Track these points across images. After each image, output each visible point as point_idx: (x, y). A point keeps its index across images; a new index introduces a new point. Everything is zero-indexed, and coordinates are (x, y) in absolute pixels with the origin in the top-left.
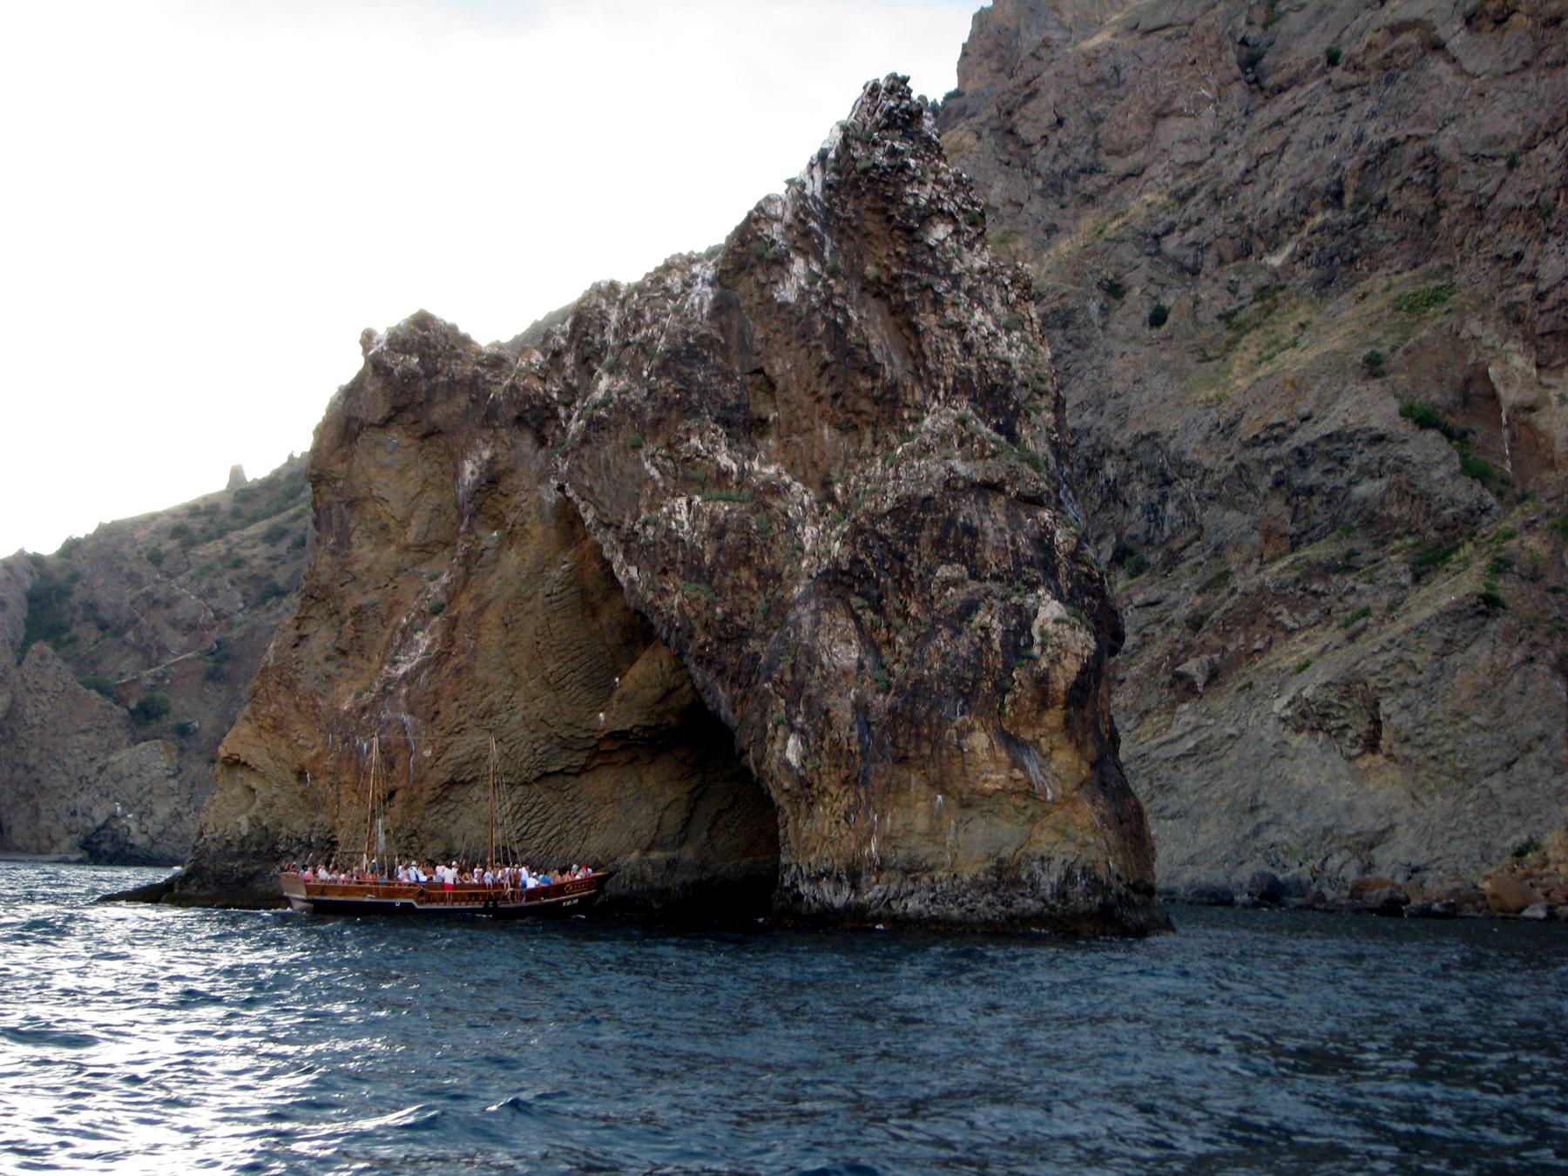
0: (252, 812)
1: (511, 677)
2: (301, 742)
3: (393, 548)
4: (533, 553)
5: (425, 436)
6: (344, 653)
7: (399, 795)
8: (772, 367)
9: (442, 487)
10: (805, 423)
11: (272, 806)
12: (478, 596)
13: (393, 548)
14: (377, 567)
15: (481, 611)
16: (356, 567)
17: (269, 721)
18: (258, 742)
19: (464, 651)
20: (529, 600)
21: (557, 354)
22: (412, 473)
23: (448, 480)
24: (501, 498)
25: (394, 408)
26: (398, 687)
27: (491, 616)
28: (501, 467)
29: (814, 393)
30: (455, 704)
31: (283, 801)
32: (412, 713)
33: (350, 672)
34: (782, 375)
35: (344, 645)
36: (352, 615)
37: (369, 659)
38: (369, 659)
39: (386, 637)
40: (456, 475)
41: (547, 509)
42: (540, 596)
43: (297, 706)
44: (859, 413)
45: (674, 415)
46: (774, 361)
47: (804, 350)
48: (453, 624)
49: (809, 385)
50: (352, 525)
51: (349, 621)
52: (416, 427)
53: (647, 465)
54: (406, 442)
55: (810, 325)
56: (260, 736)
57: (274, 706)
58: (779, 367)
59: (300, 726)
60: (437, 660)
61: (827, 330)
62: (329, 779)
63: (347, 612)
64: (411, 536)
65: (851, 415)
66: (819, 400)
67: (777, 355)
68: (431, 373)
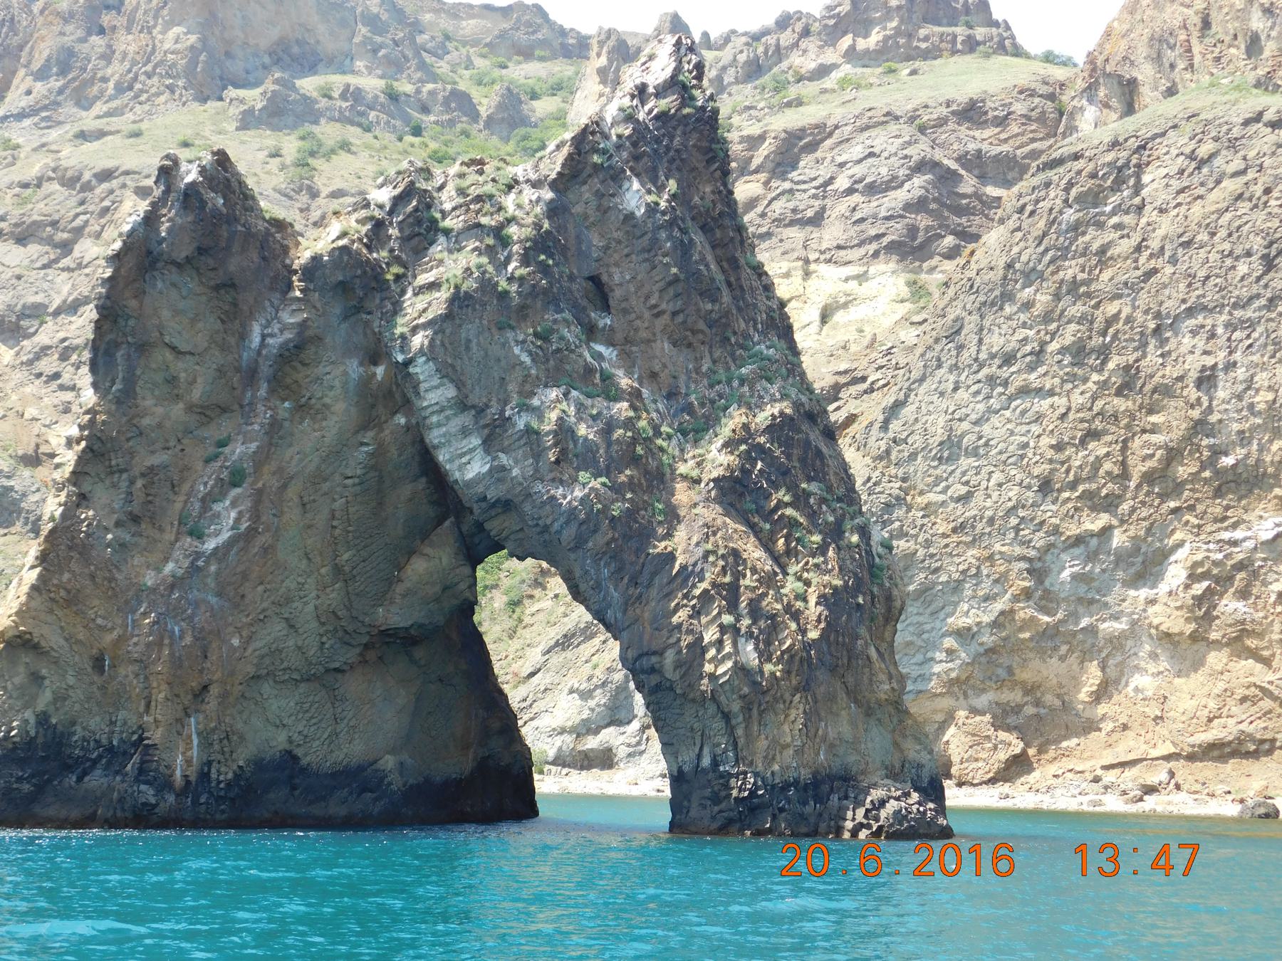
0: (41, 706)
1: (305, 561)
2: (99, 621)
3: (181, 405)
4: (334, 431)
5: (217, 288)
6: (135, 519)
7: (215, 690)
8: (610, 275)
9: (224, 348)
10: (644, 334)
11: (65, 699)
12: (280, 470)
13: (181, 405)
14: (168, 424)
15: (284, 487)
16: (146, 421)
17: (63, 593)
18: (50, 618)
19: (267, 529)
20: (325, 480)
21: (379, 225)
22: (200, 325)
23: (232, 340)
24: (299, 366)
25: (199, 249)
26: (207, 562)
27: (292, 493)
28: (310, 333)
29: (655, 306)
30: (260, 588)
31: (77, 694)
32: (219, 594)
33: (143, 542)
34: (621, 285)
35: (136, 507)
36: (143, 475)
37: (161, 529)
38: (161, 529)
39: (178, 506)
40: (243, 336)
41: (351, 386)
42: (337, 478)
43: (93, 577)
44: (694, 332)
45: (539, 304)
46: (613, 269)
47: (646, 265)
48: (259, 495)
49: (647, 297)
50: (138, 372)
51: (139, 483)
52: (212, 274)
53: (517, 350)
54: (199, 290)
55: (655, 244)
56: (51, 611)
57: (66, 576)
58: (617, 277)
59: (96, 602)
60: (242, 539)
61: (674, 248)
62: (136, 668)
63: (136, 471)
64: (196, 394)
65: (688, 333)
66: (657, 315)
67: (617, 265)
68: (231, 219)
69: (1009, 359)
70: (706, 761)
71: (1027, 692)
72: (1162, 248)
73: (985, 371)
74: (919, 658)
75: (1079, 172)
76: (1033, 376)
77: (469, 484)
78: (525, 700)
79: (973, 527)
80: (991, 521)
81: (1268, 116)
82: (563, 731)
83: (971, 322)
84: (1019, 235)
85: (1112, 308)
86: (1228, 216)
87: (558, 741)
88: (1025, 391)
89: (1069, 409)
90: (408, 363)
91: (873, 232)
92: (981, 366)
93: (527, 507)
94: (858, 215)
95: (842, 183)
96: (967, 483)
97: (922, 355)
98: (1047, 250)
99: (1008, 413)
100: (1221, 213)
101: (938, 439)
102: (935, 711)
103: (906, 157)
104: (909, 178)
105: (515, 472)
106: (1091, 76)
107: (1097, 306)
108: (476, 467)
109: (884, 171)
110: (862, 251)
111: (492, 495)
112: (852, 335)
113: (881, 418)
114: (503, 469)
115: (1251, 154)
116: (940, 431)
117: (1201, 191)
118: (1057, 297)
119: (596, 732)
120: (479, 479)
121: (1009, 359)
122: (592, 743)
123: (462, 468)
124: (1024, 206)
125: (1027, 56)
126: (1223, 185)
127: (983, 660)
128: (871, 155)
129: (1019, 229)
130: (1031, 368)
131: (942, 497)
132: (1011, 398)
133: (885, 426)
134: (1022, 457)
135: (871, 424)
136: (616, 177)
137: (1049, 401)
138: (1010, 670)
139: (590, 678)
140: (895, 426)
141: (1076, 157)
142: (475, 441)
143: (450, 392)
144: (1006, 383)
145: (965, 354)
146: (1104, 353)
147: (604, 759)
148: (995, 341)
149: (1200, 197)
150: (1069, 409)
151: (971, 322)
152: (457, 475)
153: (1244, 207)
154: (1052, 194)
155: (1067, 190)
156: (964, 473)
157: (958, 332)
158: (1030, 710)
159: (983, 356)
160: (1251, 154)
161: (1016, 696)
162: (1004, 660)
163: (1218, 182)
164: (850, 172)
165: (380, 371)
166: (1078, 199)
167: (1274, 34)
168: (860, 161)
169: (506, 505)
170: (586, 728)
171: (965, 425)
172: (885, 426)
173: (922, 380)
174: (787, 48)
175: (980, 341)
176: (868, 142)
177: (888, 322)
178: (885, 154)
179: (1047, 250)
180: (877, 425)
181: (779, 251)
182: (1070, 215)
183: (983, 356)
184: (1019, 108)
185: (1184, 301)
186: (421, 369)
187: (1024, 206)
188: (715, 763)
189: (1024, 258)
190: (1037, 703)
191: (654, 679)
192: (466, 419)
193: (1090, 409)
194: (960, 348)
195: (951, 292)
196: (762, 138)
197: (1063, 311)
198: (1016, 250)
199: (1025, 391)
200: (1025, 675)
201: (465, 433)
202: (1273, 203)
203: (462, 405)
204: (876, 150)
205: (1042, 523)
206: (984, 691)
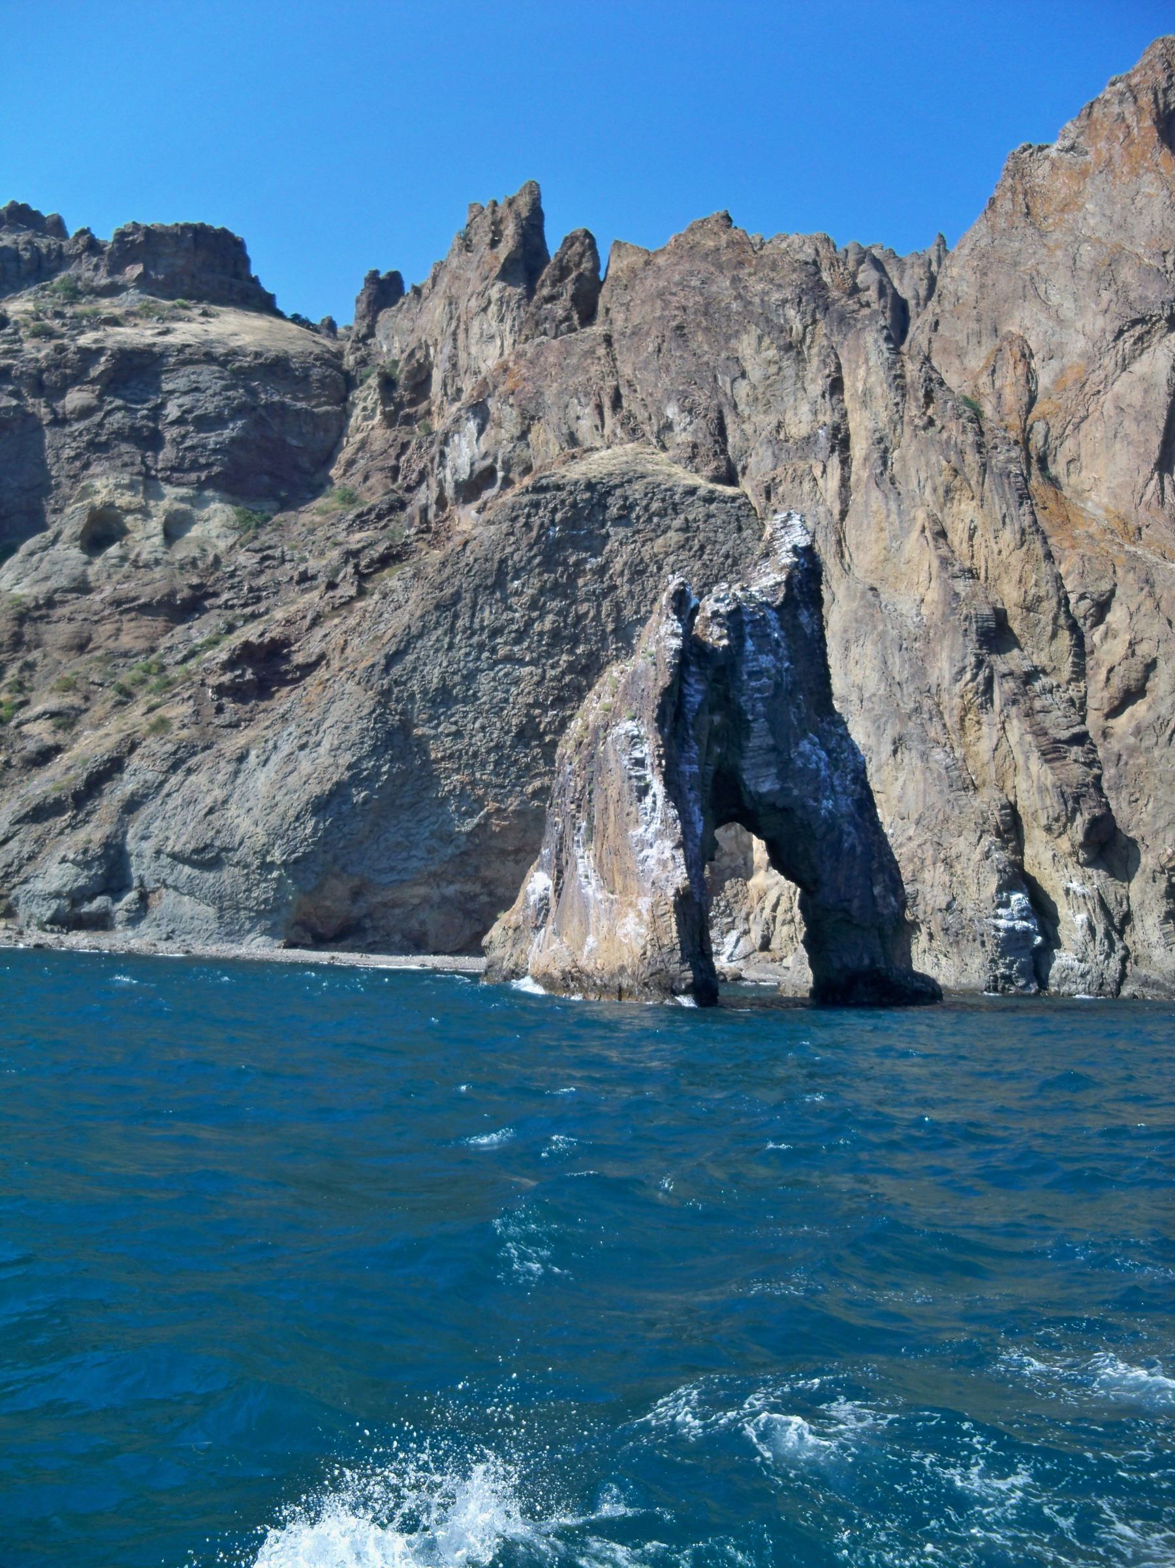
69: (496, 632)
70: (866, 961)
71: (484, 885)
72: (622, 572)
73: (475, 639)
74: (404, 854)
75: (563, 502)
76: (516, 649)
77: (761, 795)
78: (10, 865)
79: (460, 757)
80: (475, 755)
81: (702, 492)
82: (57, 895)
83: (467, 598)
84: (512, 539)
85: (583, 608)
86: (672, 558)
87: (54, 904)
88: (509, 659)
89: (543, 677)
90: (754, 720)
91: (202, 461)
92: (473, 634)
93: (799, 813)
94: (188, 443)
95: (172, 411)
96: (456, 723)
97: (422, 616)
98: (535, 556)
99: (492, 674)
100: (667, 554)
101: (434, 686)
102: (413, 897)
103: (228, 398)
104: (233, 418)
105: (796, 792)
106: (479, 396)
107: (570, 605)
108: (765, 787)
109: (211, 407)
110: (193, 476)
111: (780, 803)
112: (196, 553)
113: (383, 661)
114: (790, 789)
115: (690, 517)
116: (435, 680)
117: (652, 535)
118: (542, 591)
119: (91, 899)
120: (770, 792)
121: (496, 632)
122: (87, 908)
123: (756, 784)
124: (517, 517)
125: (280, 315)
126: (669, 534)
127: (458, 860)
128: (197, 389)
129: (512, 534)
130: (518, 641)
131: (433, 732)
132: (496, 663)
133: (387, 669)
134: (502, 709)
135: (373, 666)
136: (797, 607)
137: (528, 669)
138: (477, 869)
139: (85, 851)
140: (396, 670)
141: (559, 488)
142: (774, 770)
143: (770, 741)
144: (494, 650)
145: (460, 623)
146: (575, 641)
147: (101, 922)
148: (487, 616)
149: (651, 540)
150: (543, 677)
151: (467, 598)
152: (752, 788)
153: (684, 555)
154: (541, 513)
155: (554, 511)
156: (453, 715)
157: (455, 604)
158: (484, 899)
159: (476, 626)
160: (690, 517)
161: (476, 888)
162: (473, 861)
163: (664, 532)
164: (180, 401)
165: (717, 719)
166: (564, 521)
167: (690, 428)
168: (186, 393)
169: (786, 811)
170: (79, 896)
171: (457, 678)
172: (387, 669)
173: (420, 636)
174: (70, 256)
175: (473, 616)
176: (193, 377)
177: (222, 545)
178: (210, 392)
179: (535, 556)
180: (378, 669)
181: (119, 462)
182: (555, 532)
183: (476, 626)
184: (316, 373)
185: (636, 613)
186: (759, 726)
187: (517, 517)
188: (873, 961)
189: (516, 557)
190: (490, 894)
191: (840, 915)
192: (772, 757)
193: (560, 681)
194: (456, 617)
195: (448, 571)
196: (100, 351)
197: (545, 603)
198: (508, 550)
199: (509, 659)
200: (487, 873)
201: (768, 764)
202: (705, 557)
203: (774, 749)
204: (201, 386)
205: (516, 761)
206: (451, 883)
